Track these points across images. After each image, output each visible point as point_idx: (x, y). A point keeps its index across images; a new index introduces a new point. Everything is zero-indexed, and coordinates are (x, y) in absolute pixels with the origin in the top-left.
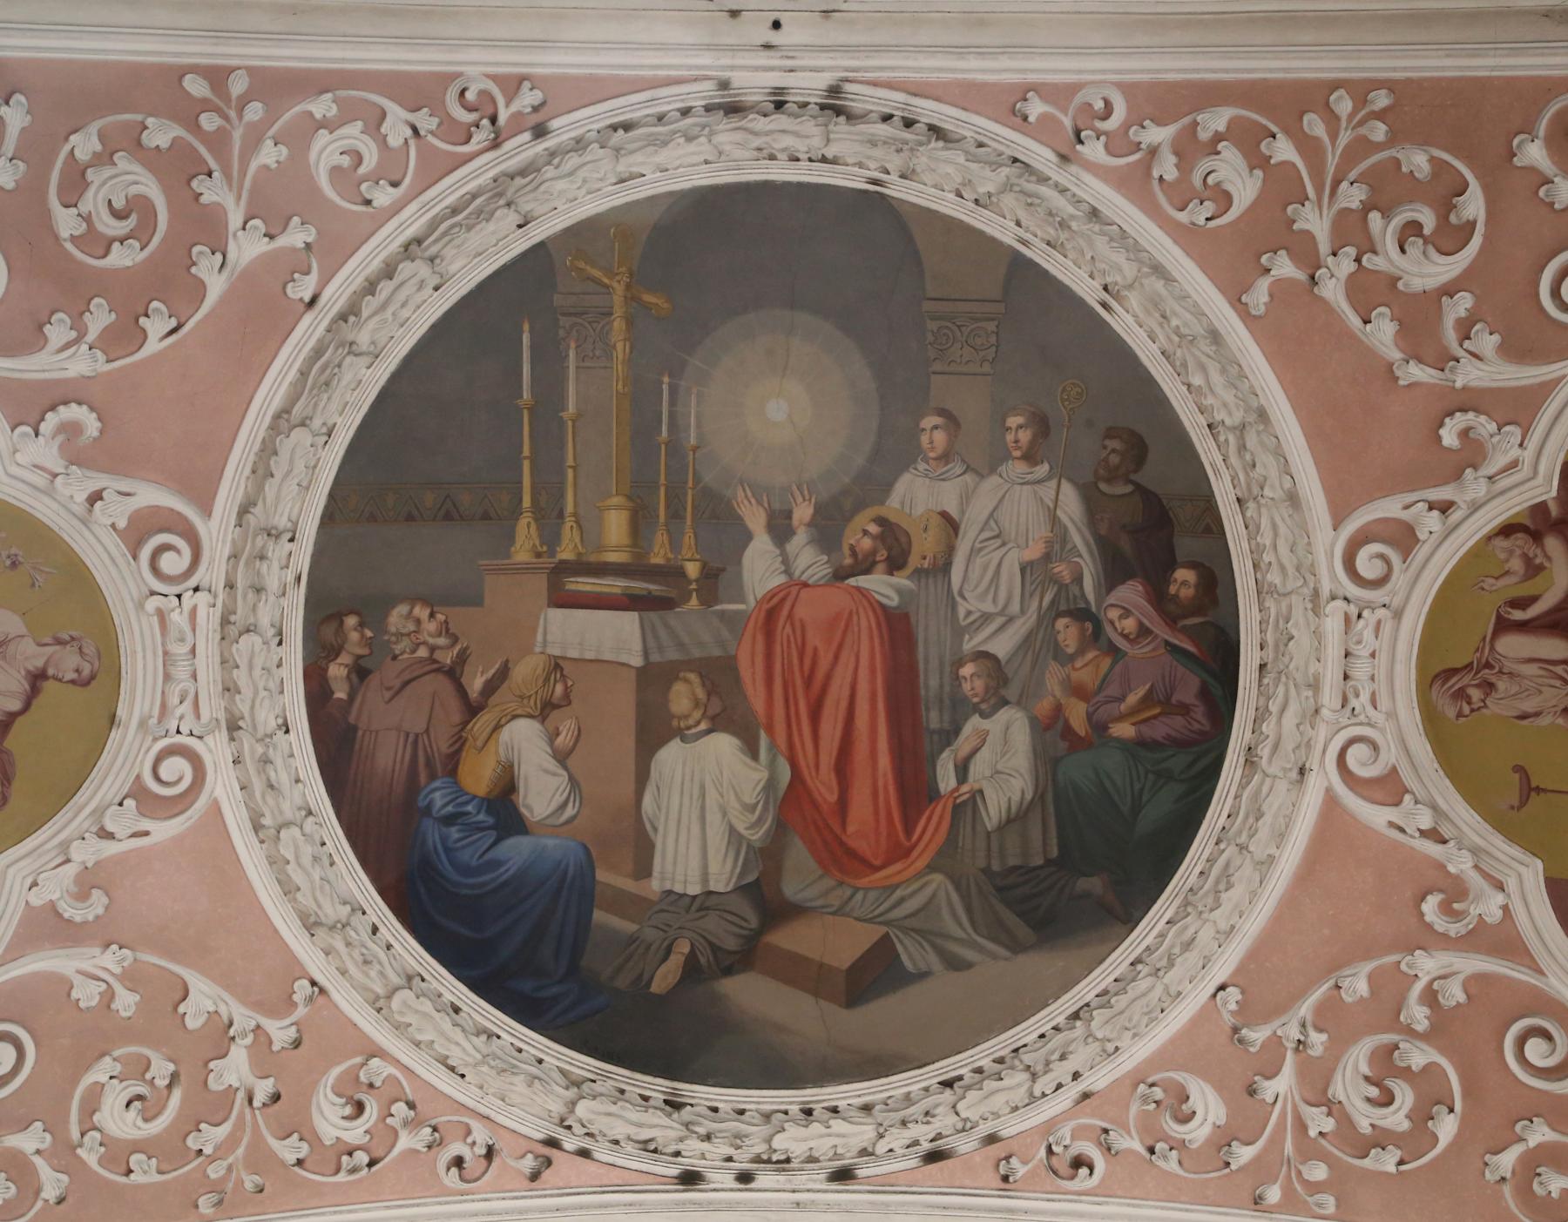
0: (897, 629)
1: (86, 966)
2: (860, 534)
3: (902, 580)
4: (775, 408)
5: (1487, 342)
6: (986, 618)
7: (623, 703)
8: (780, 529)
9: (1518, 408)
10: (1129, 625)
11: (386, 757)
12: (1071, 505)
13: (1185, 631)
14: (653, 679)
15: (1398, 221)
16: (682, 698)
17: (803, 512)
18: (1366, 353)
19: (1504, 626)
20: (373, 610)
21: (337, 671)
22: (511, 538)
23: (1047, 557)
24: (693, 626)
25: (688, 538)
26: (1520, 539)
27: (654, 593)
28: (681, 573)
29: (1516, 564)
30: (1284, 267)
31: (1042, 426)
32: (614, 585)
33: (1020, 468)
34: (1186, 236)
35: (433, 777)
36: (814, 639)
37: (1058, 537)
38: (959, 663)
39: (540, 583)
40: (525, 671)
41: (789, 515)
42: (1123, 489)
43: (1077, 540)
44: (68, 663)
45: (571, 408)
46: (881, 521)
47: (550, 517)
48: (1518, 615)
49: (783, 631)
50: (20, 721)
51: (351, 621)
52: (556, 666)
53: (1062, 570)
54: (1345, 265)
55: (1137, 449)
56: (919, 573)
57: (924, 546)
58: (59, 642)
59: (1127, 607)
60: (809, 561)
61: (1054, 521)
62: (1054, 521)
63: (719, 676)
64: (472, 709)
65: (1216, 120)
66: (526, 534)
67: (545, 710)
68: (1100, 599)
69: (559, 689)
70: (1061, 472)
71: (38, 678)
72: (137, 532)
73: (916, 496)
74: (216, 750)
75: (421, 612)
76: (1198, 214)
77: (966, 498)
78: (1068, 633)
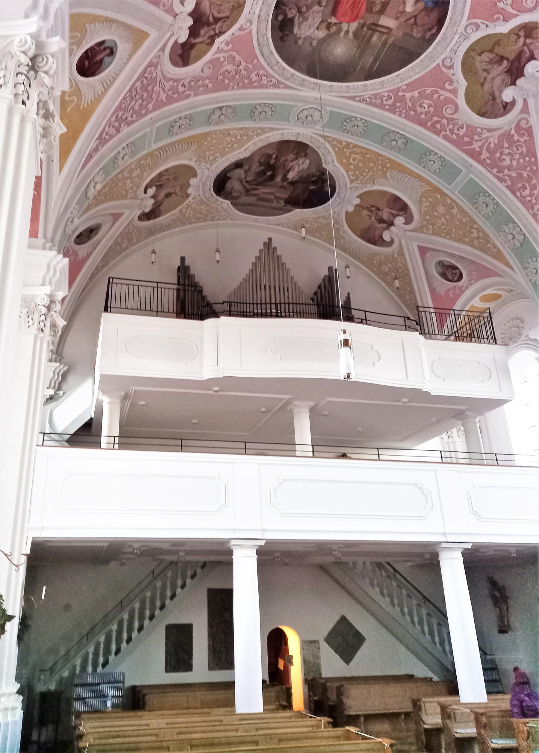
0: (334, 13)
1: (506, 6)
2: (334, 29)
3: (330, 21)
4: (340, 50)
5: (222, 59)
6: (318, 13)
7: (388, 11)
8: (347, 32)
9: (219, 51)
10: (292, 10)
11: (435, 15)
12: (296, 30)
13: (282, 9)
14: (381, 12)
15: (231, 74)
16: (377, 8)
17: (342, 34)
18: (240, 55)
19: (228, 17)
20: (423, 38)
21: (434, 31)
22: (393, 41)
23: (303, 22)
24: (370, 19)
25: (364, 33)
26: (222, 31)
27: (374, 27)
28: (367, 28)
29: (224, 27)
30: (250, 66)
31: (296, 42)
32: (380, 29)
33: (303, 36)
34: (263, 68)
35: (429, 8)
36: (349, 13)
37: (300, 24)
38: (325, 6)
39: (392, 33)
40: (403, 19)
41: (345, 34)
42: (286, 33)
43: (296, 24)
44: (473, 54)
45: (373, 58)
46: (329, 30)
47: (385, 43)
48: (225, 19)
49: (355, 15)
50: (487, 50)
51: (427, 38)
52: (397, 19)
53: (301, 19)
54: (241, 67)
55: (282, 39)
56: (326, 21)
57: (324, 25)
58: (473, 57)
59: (292, 13)
60: (345, 26)
61: (299, 28)
62: (299, 28)
63: (369, 10)
64: (415, 17)
65: (256, 84)
66: (390, 41)
67: (403, 12)
68: (296, 16)
69: (399, 15)
70: (295, 36)
71: (480, 54)
72: (451, 67)
73: (321, 34)
74: (461, 29)
75: (415, 35)
76: (262, 72)
77: (314, 32)
78: (304, 9)
